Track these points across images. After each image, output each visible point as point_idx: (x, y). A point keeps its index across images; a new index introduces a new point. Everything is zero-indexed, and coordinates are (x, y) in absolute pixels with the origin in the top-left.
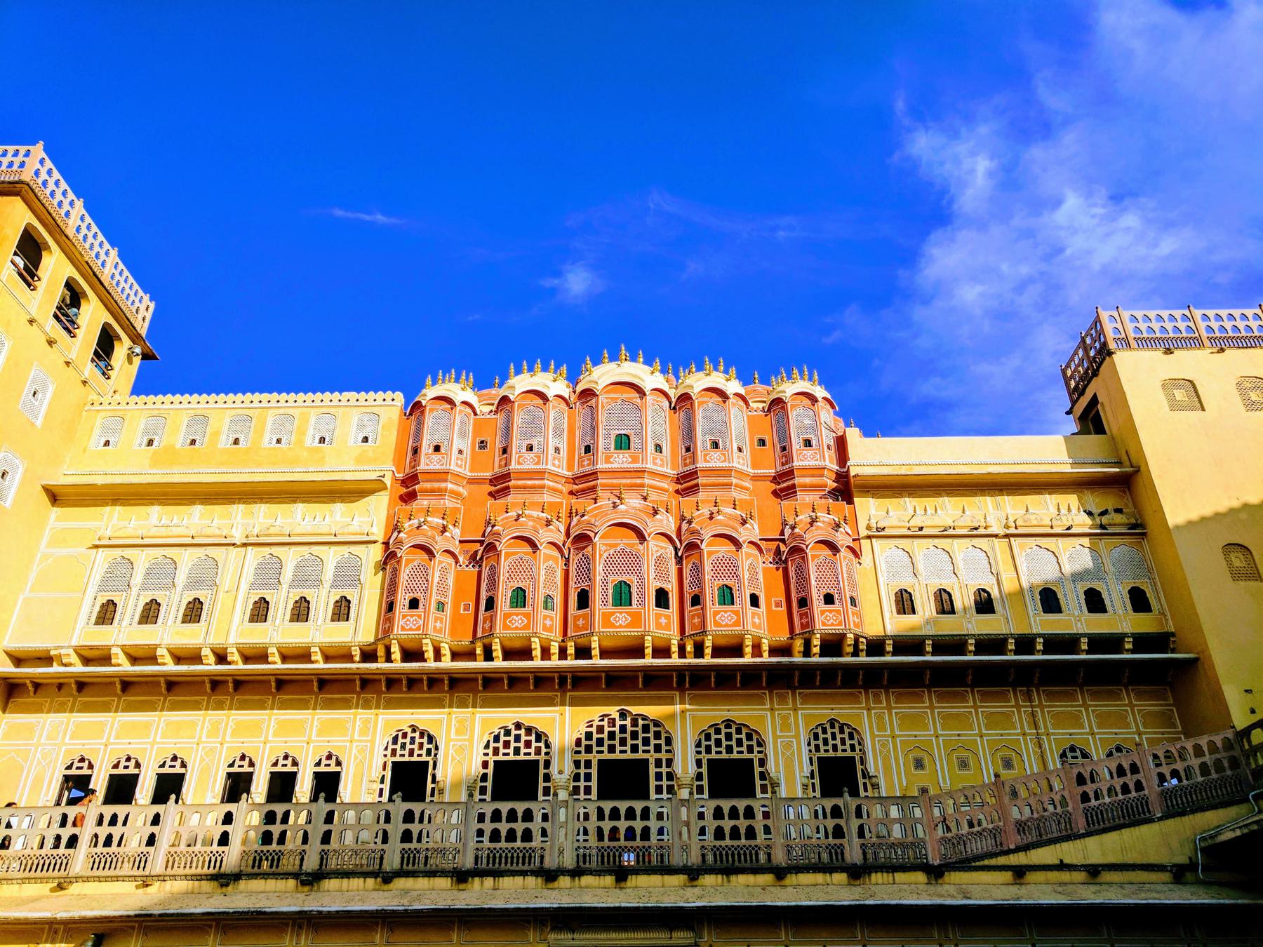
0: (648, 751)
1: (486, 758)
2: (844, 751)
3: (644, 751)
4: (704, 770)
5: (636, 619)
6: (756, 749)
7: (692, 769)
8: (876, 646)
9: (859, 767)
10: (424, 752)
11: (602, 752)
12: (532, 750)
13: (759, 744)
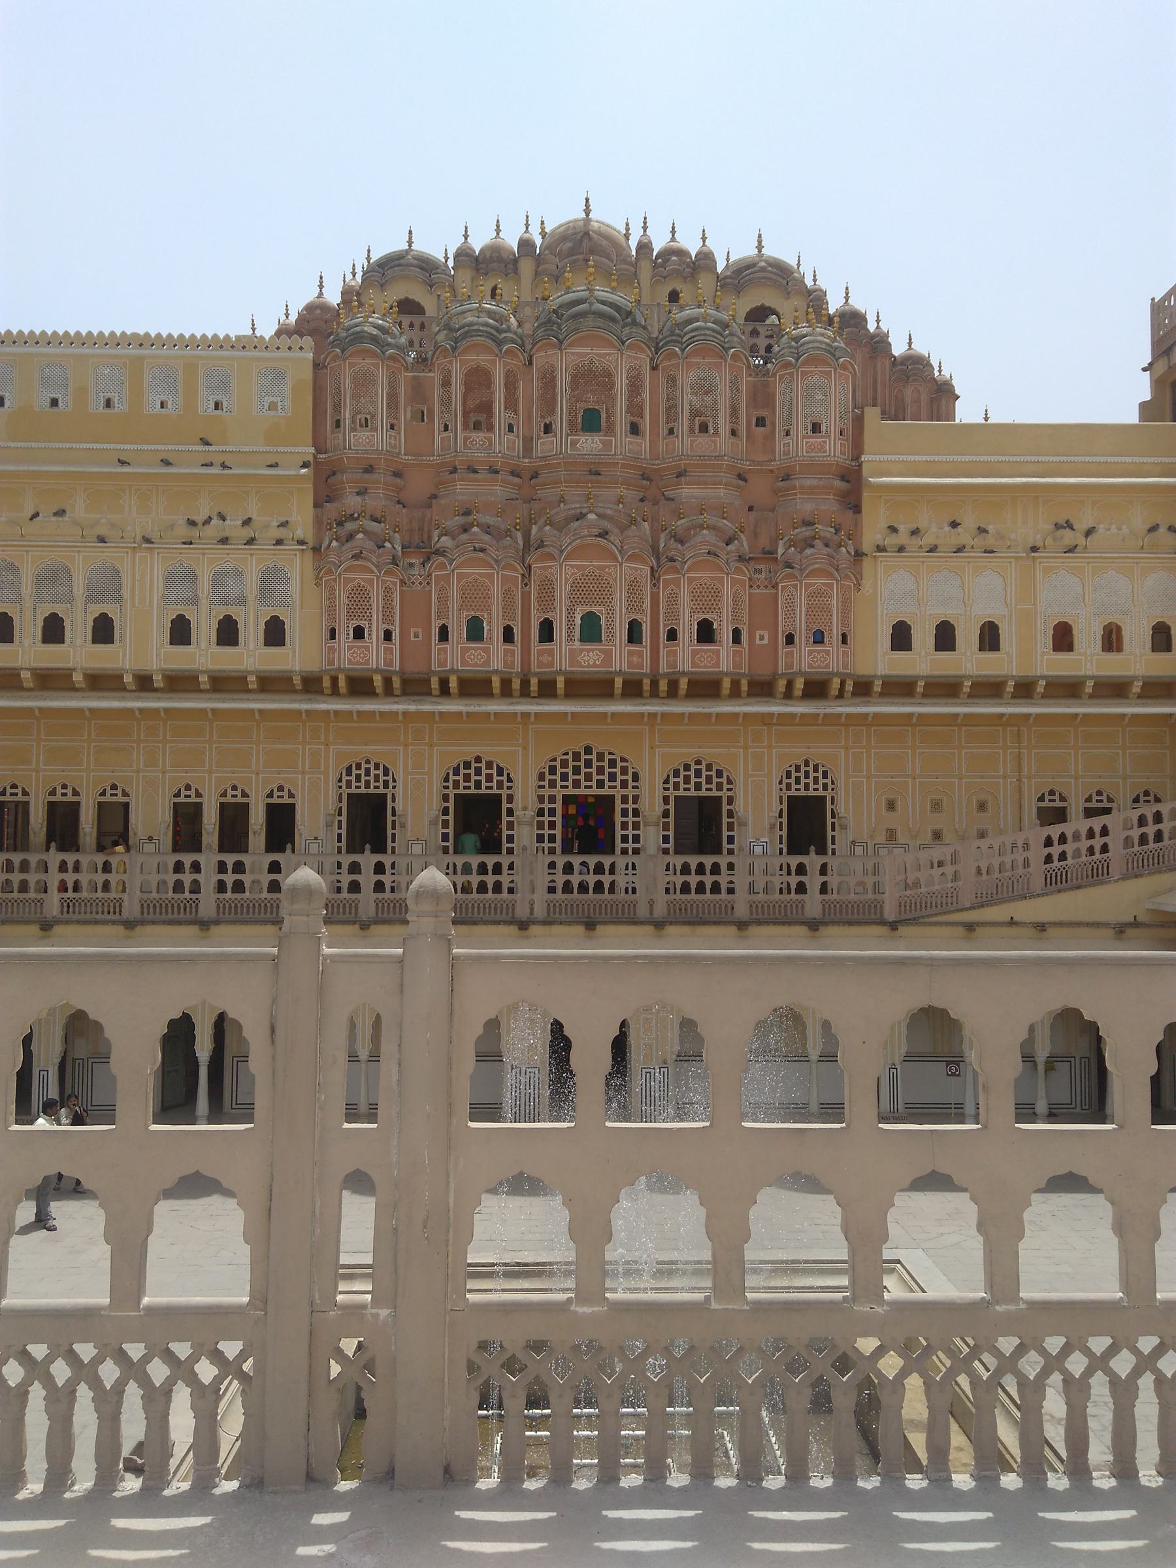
0: (615, 787)
1: (446, 791)
2: (815, 790)
3: (610, 787)
4: (671, 807)
5: (608, 654)
6: (726, 786)
7: (659, 807)
8: (863, 688)
9: (829, 806)
10: (381, 784)
11: (567, 787)
12: (494, 784)
13: (729, 782)
